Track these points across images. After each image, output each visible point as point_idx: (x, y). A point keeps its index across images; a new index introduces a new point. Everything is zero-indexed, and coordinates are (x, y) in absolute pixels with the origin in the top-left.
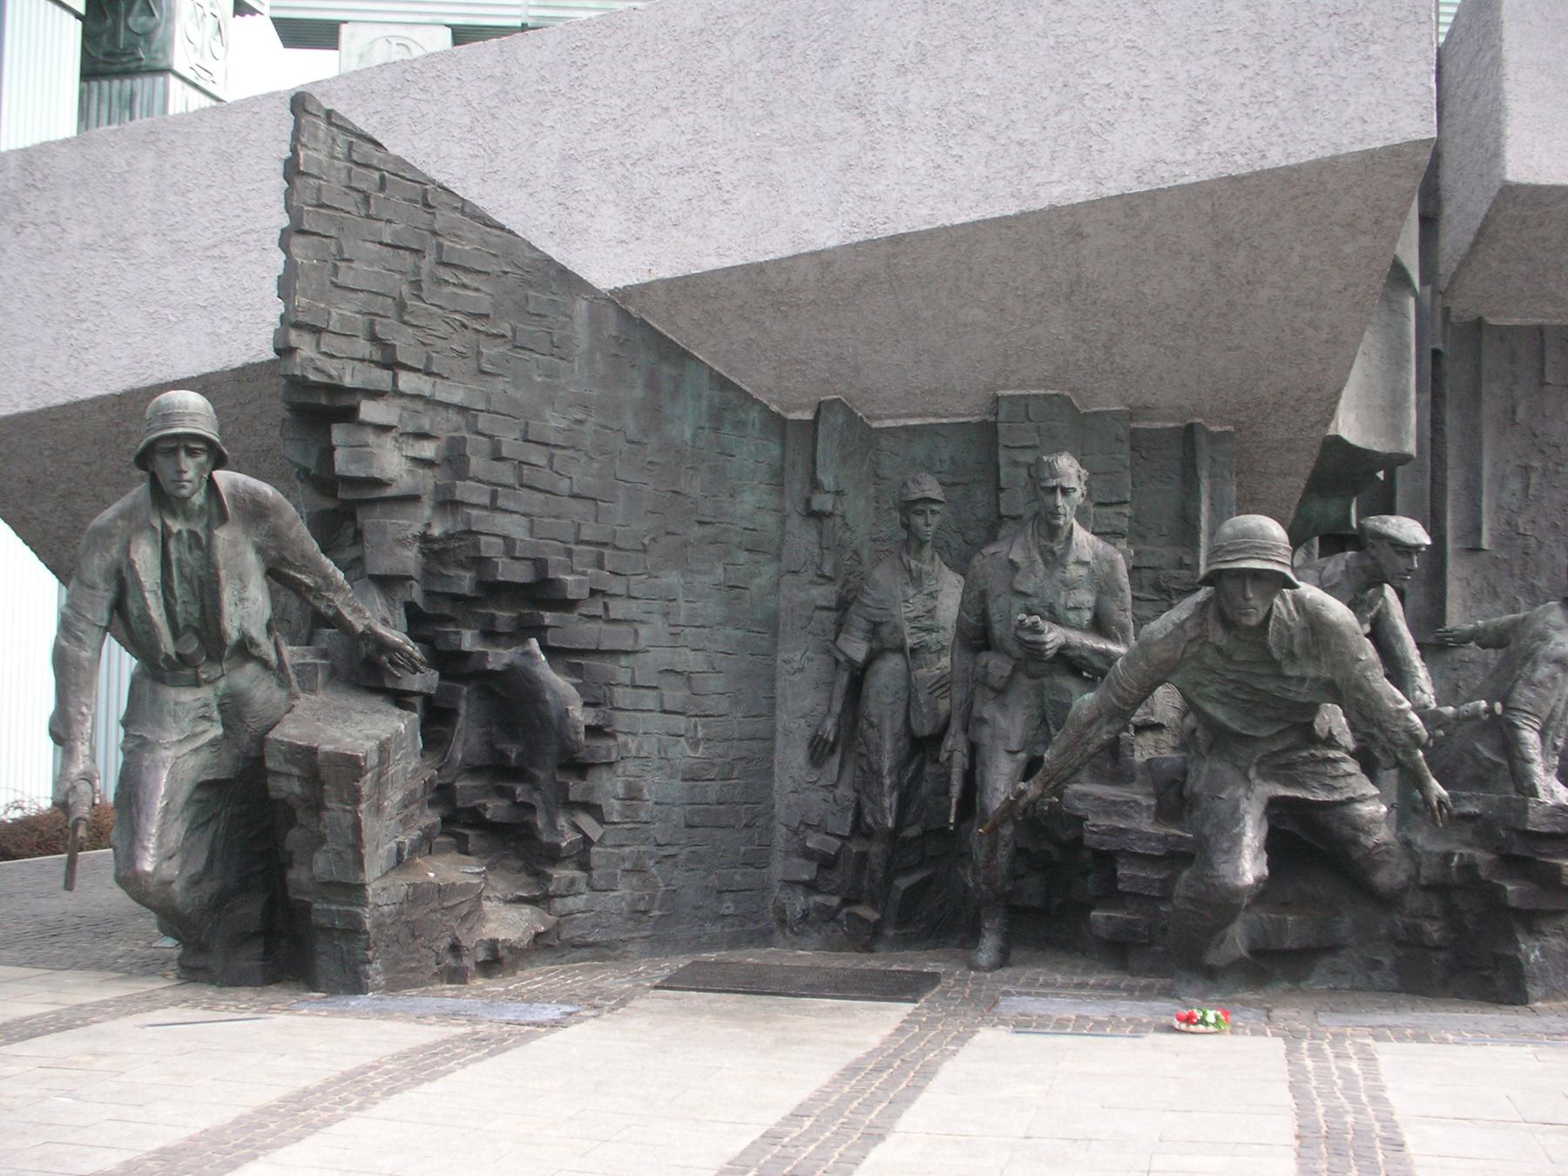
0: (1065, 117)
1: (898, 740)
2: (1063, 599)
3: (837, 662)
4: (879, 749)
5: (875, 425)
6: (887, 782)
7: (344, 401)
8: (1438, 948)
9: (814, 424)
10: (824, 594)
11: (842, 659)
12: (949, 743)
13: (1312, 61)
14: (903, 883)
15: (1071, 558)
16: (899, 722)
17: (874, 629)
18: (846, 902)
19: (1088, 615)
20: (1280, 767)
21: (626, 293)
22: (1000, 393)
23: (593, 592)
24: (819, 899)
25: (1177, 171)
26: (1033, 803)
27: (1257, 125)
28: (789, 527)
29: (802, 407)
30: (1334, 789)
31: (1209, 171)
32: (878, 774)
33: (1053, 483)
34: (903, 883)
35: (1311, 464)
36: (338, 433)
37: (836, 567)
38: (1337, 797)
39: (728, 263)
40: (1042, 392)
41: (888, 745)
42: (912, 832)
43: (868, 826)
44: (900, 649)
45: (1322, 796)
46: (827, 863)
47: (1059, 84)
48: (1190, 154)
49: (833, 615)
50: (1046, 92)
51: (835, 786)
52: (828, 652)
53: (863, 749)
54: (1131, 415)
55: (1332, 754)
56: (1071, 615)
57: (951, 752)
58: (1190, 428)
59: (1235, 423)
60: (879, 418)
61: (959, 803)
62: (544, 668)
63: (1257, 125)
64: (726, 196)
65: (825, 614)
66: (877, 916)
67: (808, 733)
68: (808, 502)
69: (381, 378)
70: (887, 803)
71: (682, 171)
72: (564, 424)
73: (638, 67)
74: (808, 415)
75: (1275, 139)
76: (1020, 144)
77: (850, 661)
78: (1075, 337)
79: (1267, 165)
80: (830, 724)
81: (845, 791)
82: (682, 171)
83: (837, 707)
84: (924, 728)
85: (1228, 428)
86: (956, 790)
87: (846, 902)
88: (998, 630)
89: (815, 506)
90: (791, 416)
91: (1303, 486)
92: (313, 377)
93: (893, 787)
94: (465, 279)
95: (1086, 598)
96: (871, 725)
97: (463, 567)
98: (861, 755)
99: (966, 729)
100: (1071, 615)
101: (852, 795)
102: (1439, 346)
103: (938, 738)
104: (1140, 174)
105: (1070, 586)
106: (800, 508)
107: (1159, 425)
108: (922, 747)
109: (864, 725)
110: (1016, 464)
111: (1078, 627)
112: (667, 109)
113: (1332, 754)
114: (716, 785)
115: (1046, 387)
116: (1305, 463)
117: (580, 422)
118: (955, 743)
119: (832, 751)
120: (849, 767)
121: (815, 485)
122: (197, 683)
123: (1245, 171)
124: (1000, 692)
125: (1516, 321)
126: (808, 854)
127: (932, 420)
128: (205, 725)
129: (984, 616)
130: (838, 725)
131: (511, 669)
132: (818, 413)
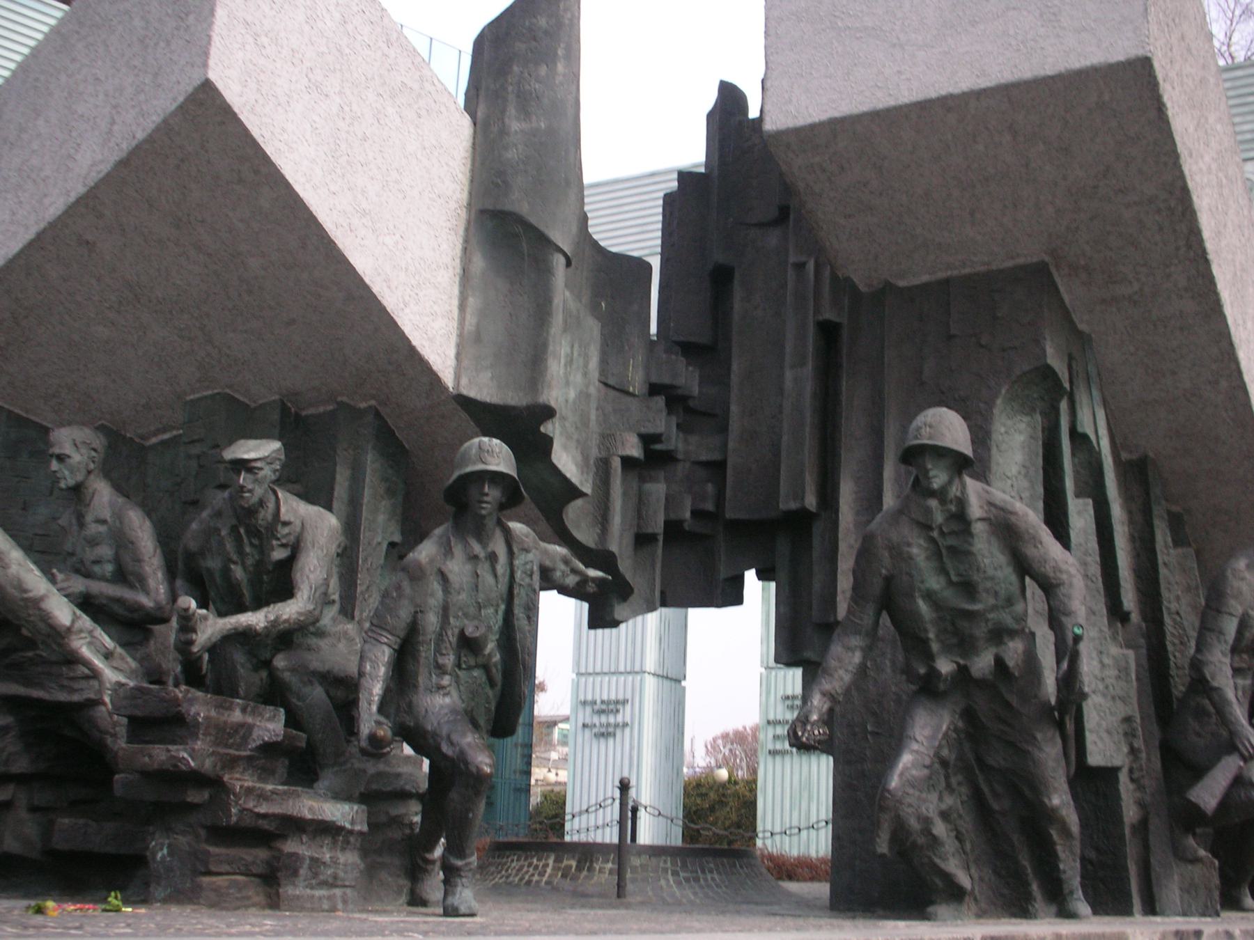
2: (90, 554)
15: (89, 518)
19: (109, 568)
30: (72, 691)
38: (76, 698)
40: (210, 392)
45: (62, 697)
56: (97, 569)
95: (106, 551)
100: (97, 569)
102: (829, 315)
104: (85, 185)
105: (93, 542)
107: (321, 409)
110: (189, 457)
111: (103, 578)
115: (208, 388)
125: (925, 278)
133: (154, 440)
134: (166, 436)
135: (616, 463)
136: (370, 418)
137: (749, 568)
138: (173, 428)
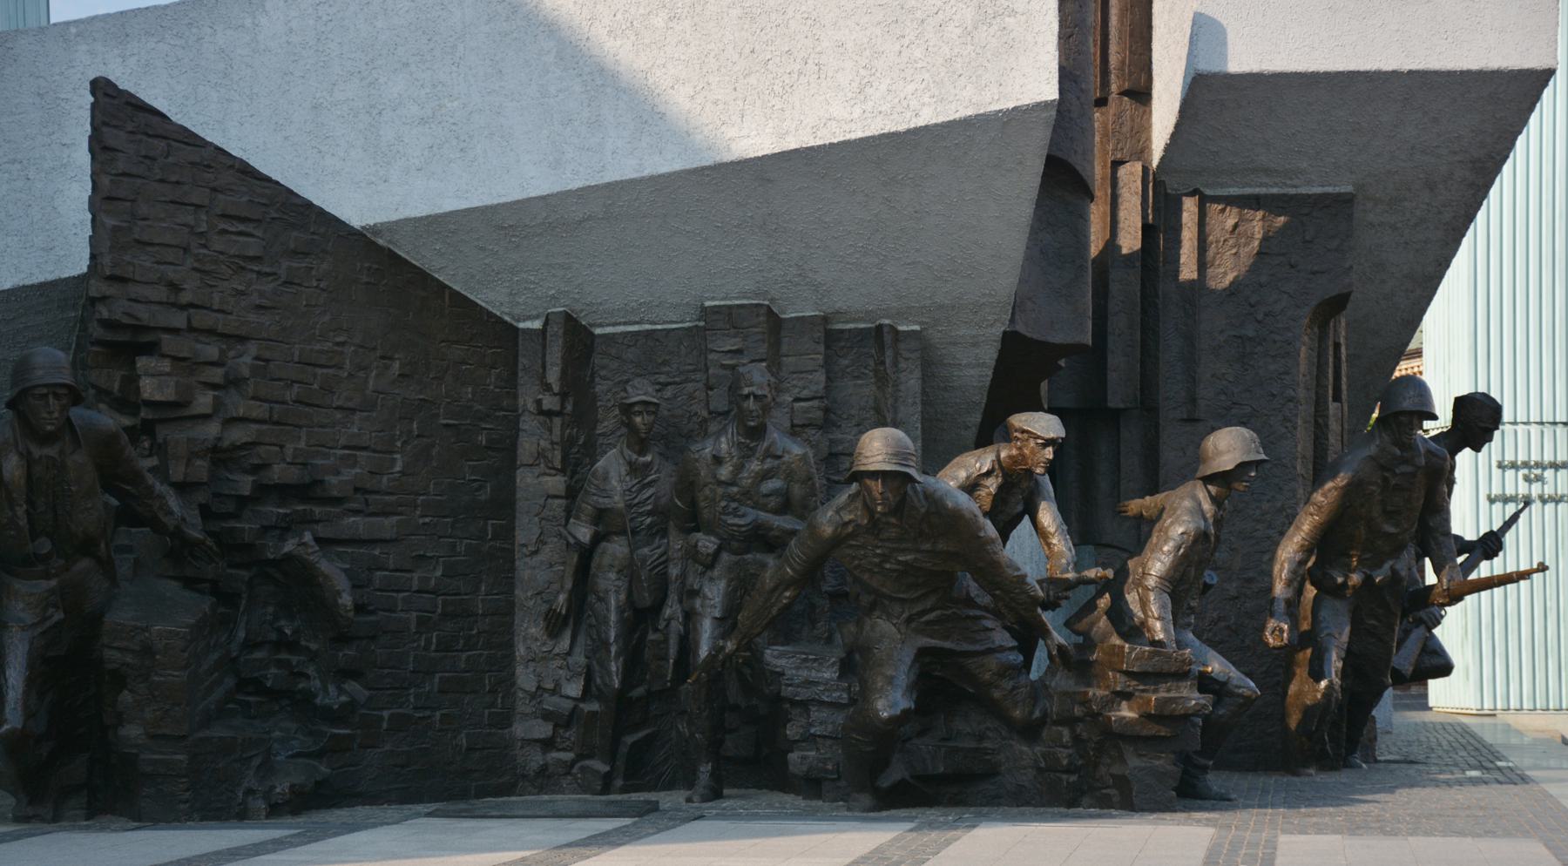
0: (752, 80)
1: (623, 612)
3: (568, 544)
4: (606, 621)
5: (598, 331)
6: (613, 649)
7: (146, 338)
8: (1068, 771)
9: (543, 331)
10: (557, 483)
11: (572, 541)
12: (667, 612)
13: (958, 31)
14: (630, 739)
16: (622, 597)
17: (600, 516)
18: (581, 757)
20: (928, 623)
21: (376, 229)
22: (708, 304)
23: (356, 490)
24: (555, 755)
25: (847, 128)
26: (730, 656)
27: (911, 88)
28: (522, 426)
29: (529, 318)
30: (975, 641)
31: (876, 127)
32: (606, 644)
33: (746, 391)
34: (630, 739)
35: (995, 356)
36: (142, 362)
37: (564, 459)
39: (464, 205)
41: (613, 617)
42: (639, 692)
43: (599, 689)
44: (623, 532)
46: (563, 721)
47: (747, 51)
48: (857, 111)
49: (562, 502)
50: (736, 57)
51: (569, 654)
52: (560, 535)
53: (593, 621)
54: (825, 319)
55: (972, 613)
57: (669, 621)
58: (880, 328)
59: (920, 323)
60: (601, 325)
61: (676, 663)
62: (314, 555)
63: (911, 88)
64: (462, 145)
65: (557, 501)
66: (607, 768)
67: (545, 607)
68: (539, 402)
69: (179, 320)
70: (614, 669)
71: (423, 121)
72: (328, 346)
73: (379, 24)
74: (537, 325)
75: (926, 100)
76: (716, 103)
77: (578, 543)
78: (771, 258)
79: (921, 122)
80: (562, 598)
81: (579, 658)
82: (423, 121)
83: (569, 585)
84: (646, 599)
85: (917, 328)
86: (673, 651)
87: (581, 757)
88: (706, 514)
89: (545, 407)
90: (521, 325)
91: (990, 373)
92: (126, 320)
93: (618, 655)
94: (241, 227)
96: (600, 599)
97: (246, 472)
98: (590, 626)
99: (681, 601)
101: (582, 660)
103: (657, 608)
106: (531, 407)
107: (851, 326)
108: (640, 617)
109: (592, 598)
110: (723, 366)
112: (407, 65)
113: (972, 613)
114: (464, 656)
117: (343, 344)
118: (672, 609)
119: (565, 623)
120: (581, 639)
121: (547, 388)
122: (47, 576)
123: (902, 128)
124: (711, 566)
126: (547, 716)
128: (51, 610)
129: (693, 503)
130: (569, 601)
131: (289, 557)
132: (546, 324)
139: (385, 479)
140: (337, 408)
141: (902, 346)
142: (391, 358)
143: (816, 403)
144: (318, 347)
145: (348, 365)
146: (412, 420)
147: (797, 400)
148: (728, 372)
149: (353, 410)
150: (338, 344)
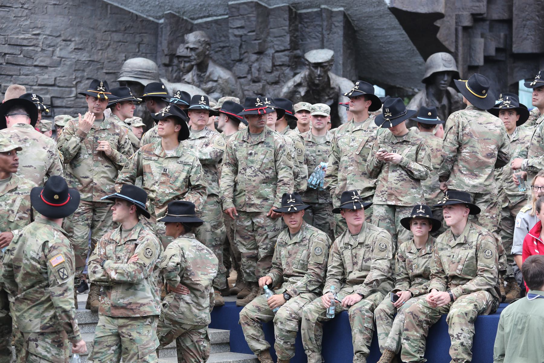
72: (27, 36)
85: (342, 9)
110: (236, 36)
116: (395, 22)
117: (38, 34)
127: (215, 18)
133: (200, 21)
134: (209, 19)
135: (460, 28)
136: (341, 18)
137: (521, 79)
138: (216, 16)
139: (65, 101)
140: (36, 66)
141: (334, 19)
142: (70, 41)
143: (287, 53)
144: (22, 36)
145: (41, 45)
146: (83, 71)
147: (277, 52)
148: (239, 39)
149: (46, 67)
150: (35, 35)
